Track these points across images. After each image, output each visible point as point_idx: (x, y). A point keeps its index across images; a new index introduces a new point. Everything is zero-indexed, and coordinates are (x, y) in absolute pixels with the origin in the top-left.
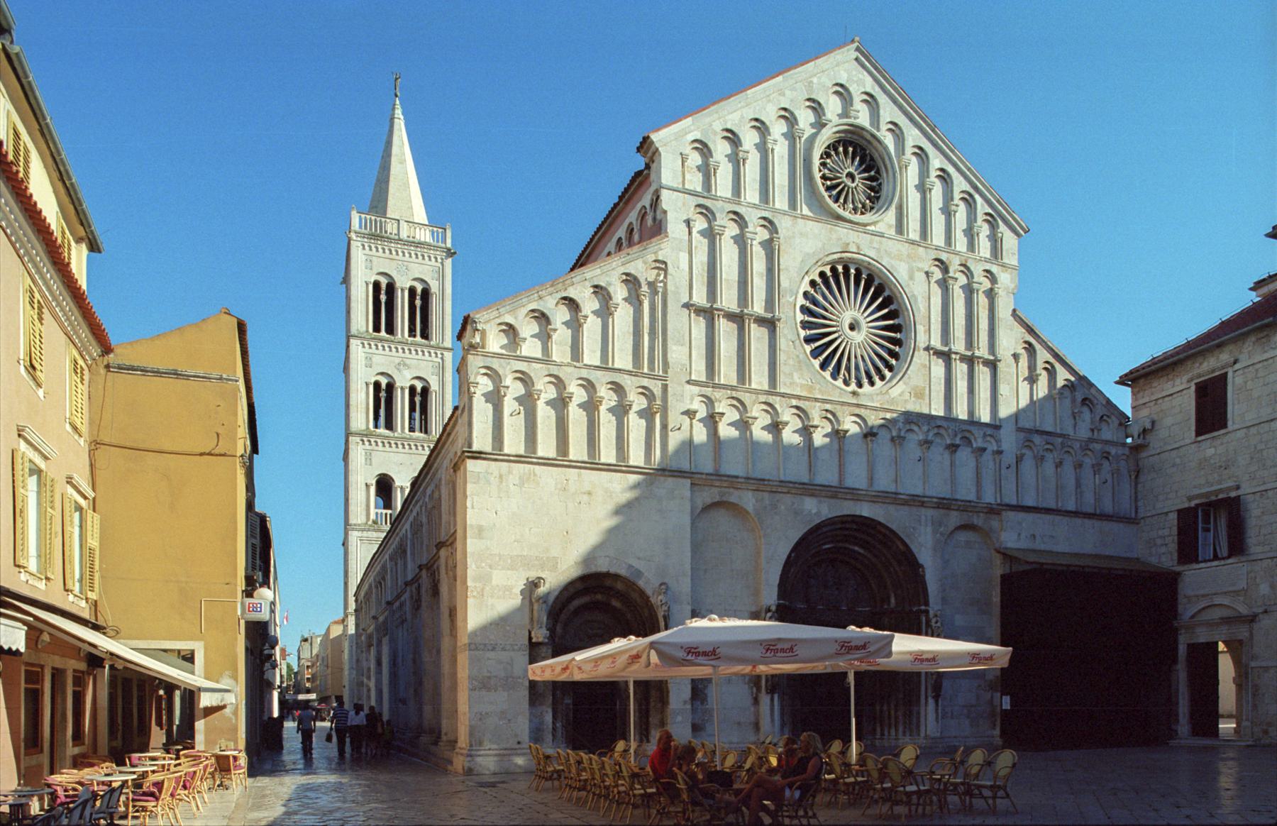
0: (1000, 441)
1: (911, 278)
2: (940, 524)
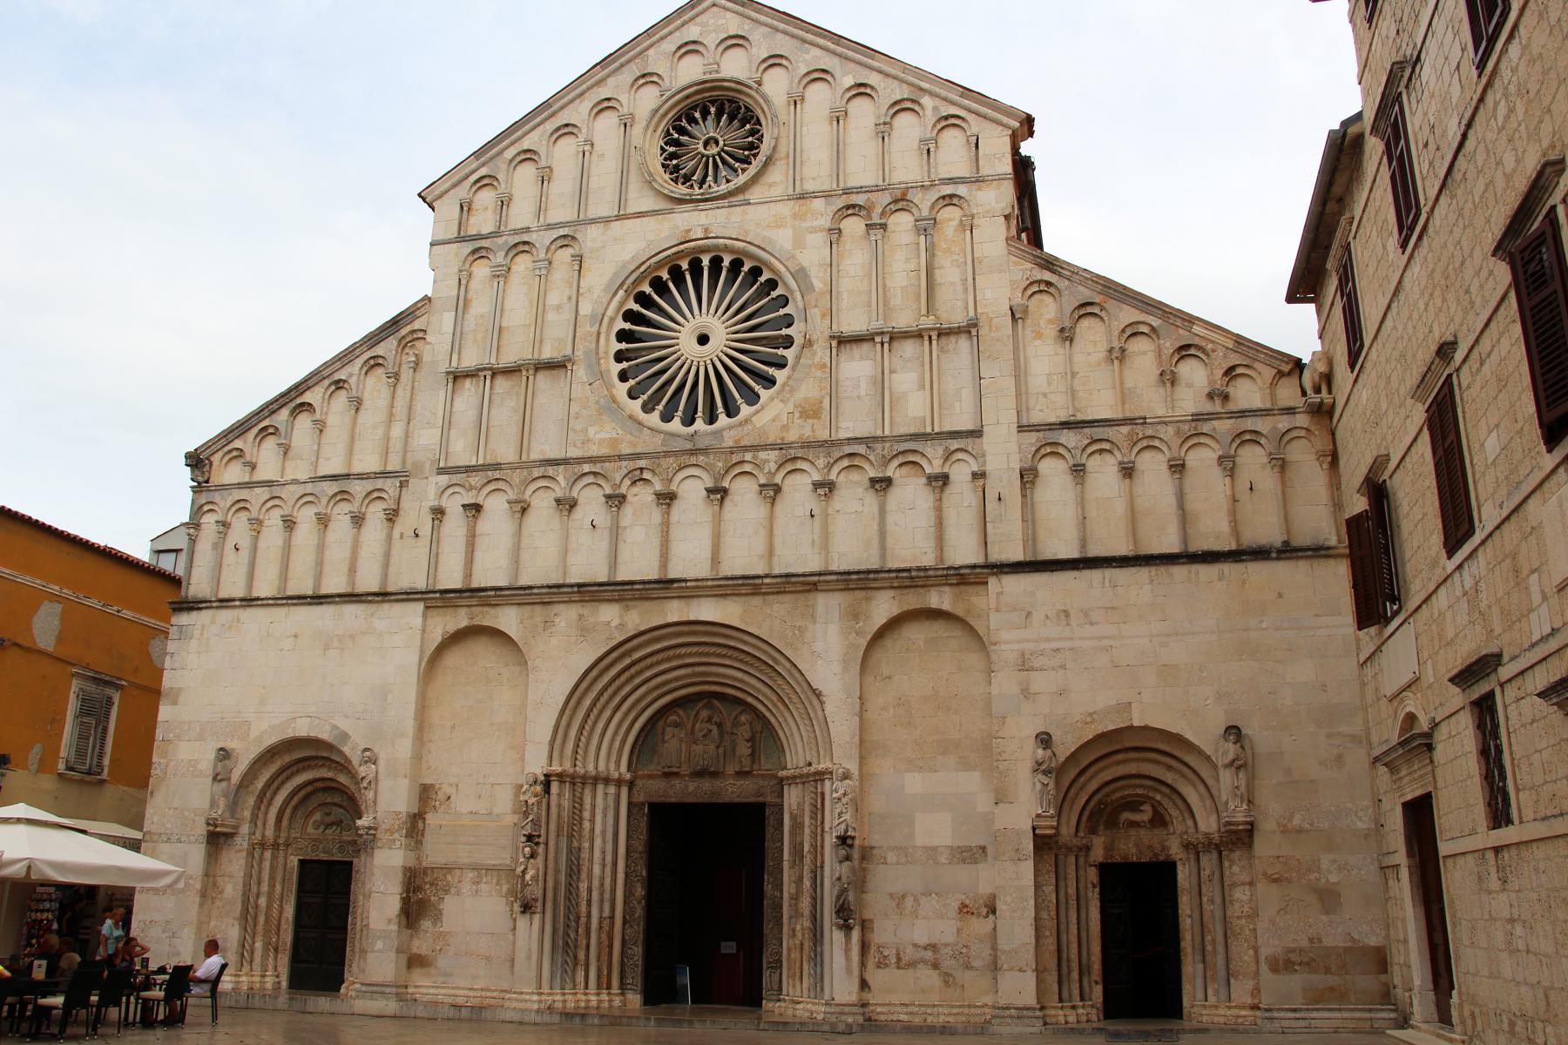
0: (984, 456)
1: (799, 243)
2: (856, 616)
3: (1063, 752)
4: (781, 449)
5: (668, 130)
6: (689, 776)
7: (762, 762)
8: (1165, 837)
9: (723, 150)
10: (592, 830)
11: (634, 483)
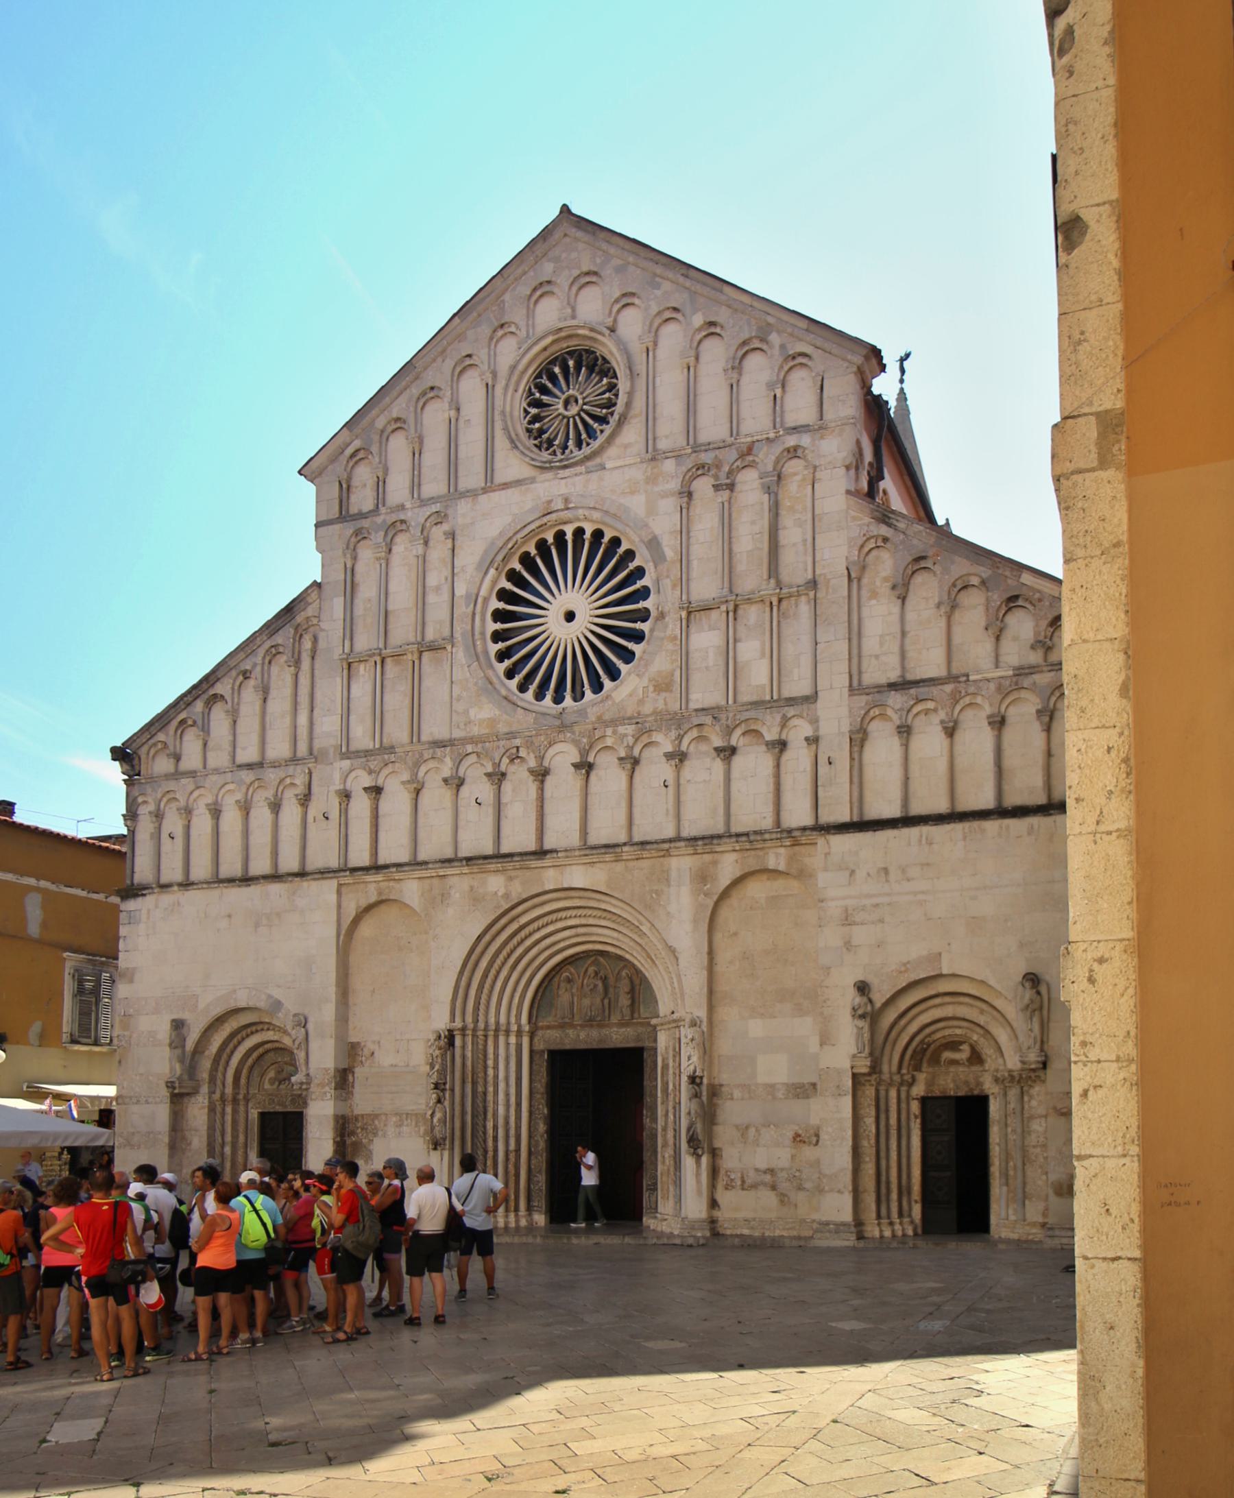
3: (879, 999)
4: (637, 723)
5: (530, 389)
6: (581, 1026)
7: (642, 1010)
8: (980, 1074)
9: (582, 410)
10: (496, 1077)
11: (512, 760)
